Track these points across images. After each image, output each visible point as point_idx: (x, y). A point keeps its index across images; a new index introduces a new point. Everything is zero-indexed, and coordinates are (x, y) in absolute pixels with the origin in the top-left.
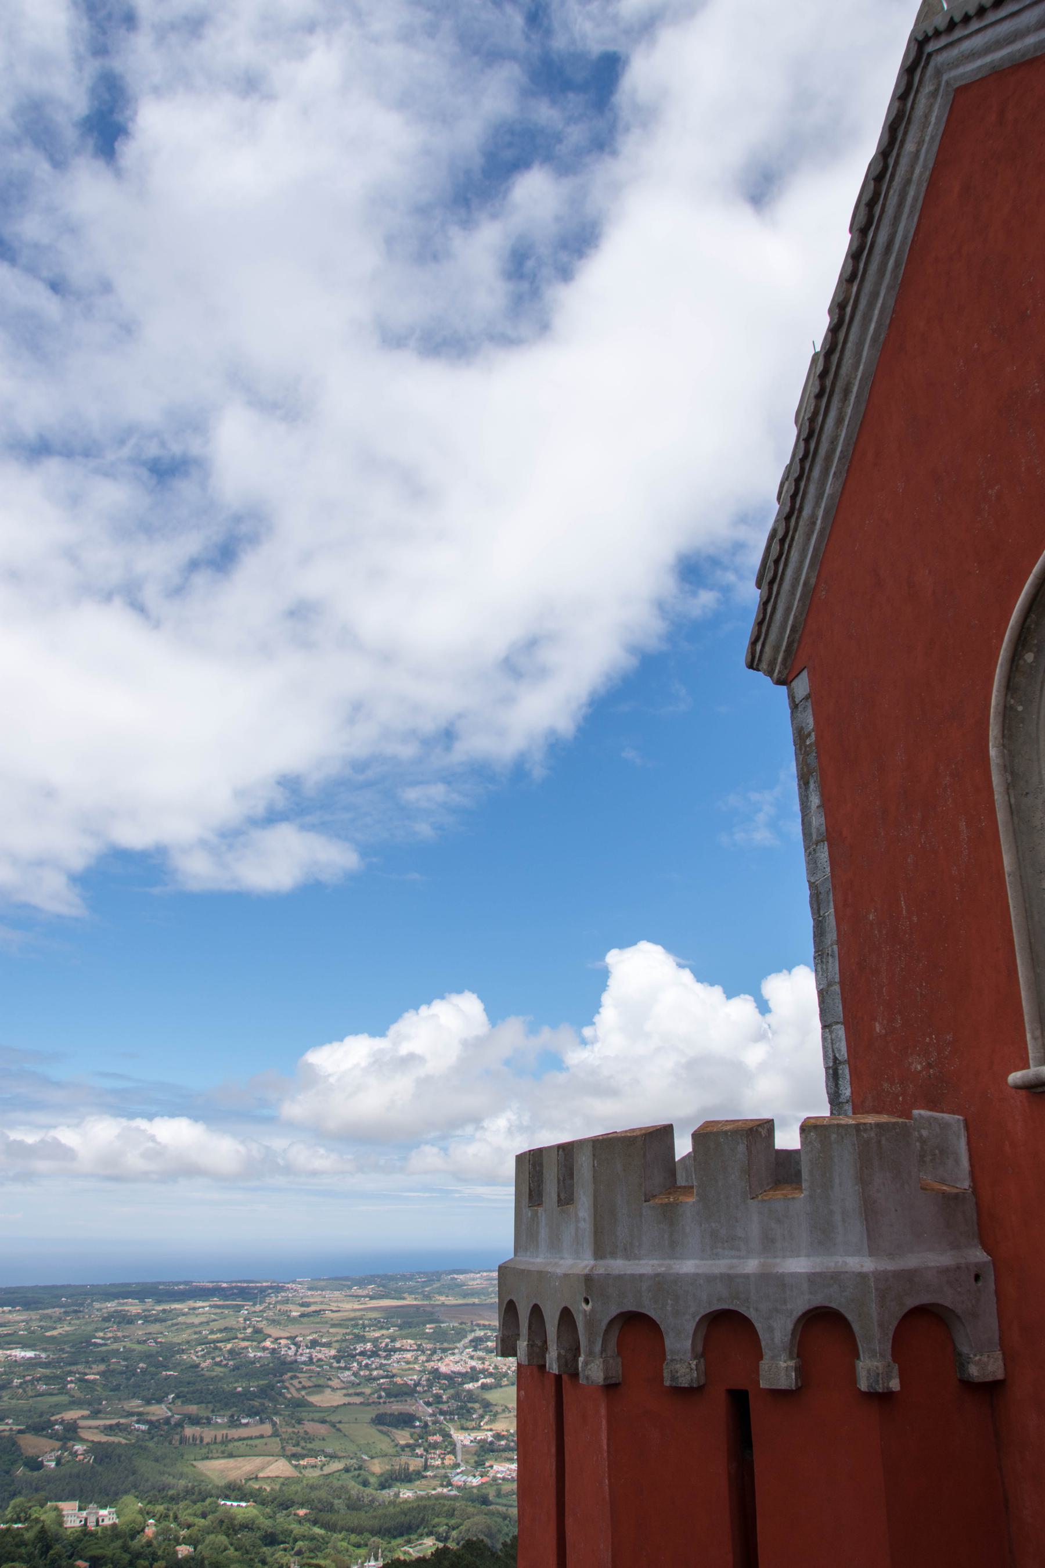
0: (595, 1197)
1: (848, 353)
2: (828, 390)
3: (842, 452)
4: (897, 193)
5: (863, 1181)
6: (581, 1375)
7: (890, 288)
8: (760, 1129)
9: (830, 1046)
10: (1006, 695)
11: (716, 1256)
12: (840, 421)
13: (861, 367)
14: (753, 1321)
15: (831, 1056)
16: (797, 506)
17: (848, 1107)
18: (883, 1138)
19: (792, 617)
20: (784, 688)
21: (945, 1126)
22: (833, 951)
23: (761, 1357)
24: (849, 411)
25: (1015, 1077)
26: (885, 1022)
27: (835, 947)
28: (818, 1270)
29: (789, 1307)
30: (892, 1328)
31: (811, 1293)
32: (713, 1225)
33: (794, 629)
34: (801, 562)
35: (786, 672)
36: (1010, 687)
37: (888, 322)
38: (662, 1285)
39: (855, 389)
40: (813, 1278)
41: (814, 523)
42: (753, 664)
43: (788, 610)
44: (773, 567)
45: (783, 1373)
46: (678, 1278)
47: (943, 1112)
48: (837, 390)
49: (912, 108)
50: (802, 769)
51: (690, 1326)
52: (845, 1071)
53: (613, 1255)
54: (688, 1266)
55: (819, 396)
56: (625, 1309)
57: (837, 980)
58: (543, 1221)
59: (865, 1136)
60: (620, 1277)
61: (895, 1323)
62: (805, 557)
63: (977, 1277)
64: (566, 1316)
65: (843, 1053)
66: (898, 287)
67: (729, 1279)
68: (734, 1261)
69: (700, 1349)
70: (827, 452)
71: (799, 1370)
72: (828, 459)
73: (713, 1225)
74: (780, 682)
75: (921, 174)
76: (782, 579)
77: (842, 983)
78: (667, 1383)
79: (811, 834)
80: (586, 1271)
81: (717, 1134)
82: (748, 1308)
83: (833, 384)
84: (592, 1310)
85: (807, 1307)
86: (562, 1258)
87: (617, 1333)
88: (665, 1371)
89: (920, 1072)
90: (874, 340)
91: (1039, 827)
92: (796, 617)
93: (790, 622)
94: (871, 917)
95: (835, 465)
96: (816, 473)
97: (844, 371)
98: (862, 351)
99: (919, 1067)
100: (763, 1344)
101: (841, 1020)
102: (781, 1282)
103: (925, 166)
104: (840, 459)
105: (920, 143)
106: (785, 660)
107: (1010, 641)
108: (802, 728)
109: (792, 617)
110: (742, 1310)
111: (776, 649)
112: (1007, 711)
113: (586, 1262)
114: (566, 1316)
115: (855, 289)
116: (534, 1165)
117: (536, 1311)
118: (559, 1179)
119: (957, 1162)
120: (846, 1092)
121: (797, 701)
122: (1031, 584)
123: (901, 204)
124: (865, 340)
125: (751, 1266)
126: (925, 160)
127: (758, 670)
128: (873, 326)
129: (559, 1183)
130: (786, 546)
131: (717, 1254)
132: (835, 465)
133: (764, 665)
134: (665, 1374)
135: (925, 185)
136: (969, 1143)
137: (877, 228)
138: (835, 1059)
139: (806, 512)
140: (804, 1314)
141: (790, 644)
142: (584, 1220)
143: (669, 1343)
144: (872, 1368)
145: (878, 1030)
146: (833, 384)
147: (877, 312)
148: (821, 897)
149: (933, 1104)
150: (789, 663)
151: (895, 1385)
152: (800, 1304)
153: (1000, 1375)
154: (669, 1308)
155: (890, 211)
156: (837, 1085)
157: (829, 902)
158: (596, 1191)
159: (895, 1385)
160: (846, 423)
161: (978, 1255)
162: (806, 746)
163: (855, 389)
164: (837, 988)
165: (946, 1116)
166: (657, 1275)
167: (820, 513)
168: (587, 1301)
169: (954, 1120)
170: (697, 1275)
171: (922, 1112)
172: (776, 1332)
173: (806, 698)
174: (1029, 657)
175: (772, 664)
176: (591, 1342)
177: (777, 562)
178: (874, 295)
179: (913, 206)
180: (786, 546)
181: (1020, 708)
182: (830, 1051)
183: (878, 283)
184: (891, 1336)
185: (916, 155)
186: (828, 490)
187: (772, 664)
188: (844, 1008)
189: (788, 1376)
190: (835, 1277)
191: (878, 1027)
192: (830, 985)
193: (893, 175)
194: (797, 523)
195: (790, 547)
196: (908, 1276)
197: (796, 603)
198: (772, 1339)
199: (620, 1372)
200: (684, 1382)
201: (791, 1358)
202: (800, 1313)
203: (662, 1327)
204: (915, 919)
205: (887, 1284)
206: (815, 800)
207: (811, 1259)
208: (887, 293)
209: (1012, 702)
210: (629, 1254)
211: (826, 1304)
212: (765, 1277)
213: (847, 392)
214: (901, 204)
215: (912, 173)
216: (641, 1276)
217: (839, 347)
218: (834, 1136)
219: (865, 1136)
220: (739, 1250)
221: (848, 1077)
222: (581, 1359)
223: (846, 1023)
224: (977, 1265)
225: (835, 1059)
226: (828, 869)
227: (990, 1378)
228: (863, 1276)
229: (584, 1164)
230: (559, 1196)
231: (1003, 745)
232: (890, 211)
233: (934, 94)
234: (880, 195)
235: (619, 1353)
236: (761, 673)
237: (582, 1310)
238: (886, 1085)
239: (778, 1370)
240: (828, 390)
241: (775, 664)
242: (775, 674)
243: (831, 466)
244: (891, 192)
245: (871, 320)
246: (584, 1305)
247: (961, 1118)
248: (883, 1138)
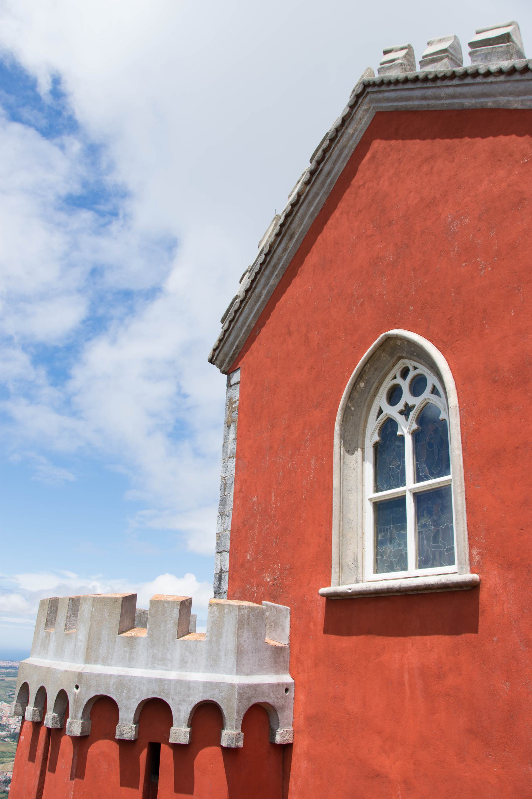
0: (90, 629)
1: (297, 218)
2: (283, 233)
3: (282, 265)
4: (339, 150)
5: (238, 635)
6: (67, 730)
7: (325, 193)
8: (186, 602)
9: (219, 562)
10: (348, 401)
11: (154, 668)
12: (285, 250)
13: (302, 227)
14: (170, 705)
15: (219, 568)
16: (254, 286)
17: (225, 595)
18: (251, 614)
19: (238, 341)
20: (225, 377)
21: (279, 611)
22: (229, 514)
23: (171, 725)
24: (291, 246)
25: (323, 590)
26: (253, 554)
27: (231, 512)
28: (209, 680)
29: (191, 699)
30: (243, 714)
31: (204, 693)
32: (155, 651)
33: (237, 347)
34: (249, 315)
35: (228, 368)
36: (350, 397)
37: (320, 209)
38: (122, 682)
39: (296, 236)
40: (207, 685)
41: (260, 297)
42: (211, 361)
43: (237, 337)
44: (233, 314)
46: (131, 679)
47: (278, 603)
48: (287, 235)
49: (355, 113)
50: (228, 418)
51: (135, 706)
52: (226, 577)
53: (96, 662)
54: (138, 672)
55: (277, 235)
56: (99, 694)
57: (229, 529)
58: (53, 638)
59: (242, 612)
60: (99, 675)
61: (245, 711)
62: (252, 312)
63: (287, 690)
64: (62, 696)
65: (226, 567)
66: (328, 194)
67: (160, 681)
68: (164, 671)
69: (137, 719)
70: (275, 263)
71: (192, 734)
72: (275, 267)
73: (155, 651)
74: (224, 372)
75: (353, 144)
76: (237, 321)
77: (232, 531)
78: (117, 737)
79: (227, 453)
80: (80, 670)
81: (164, 602)
82: (168, 698)
83: (286, 231)
84: (80, 693)
86: (63, 661)
87: (91, 707)
88: (117, 730)
89: (269, 582)
90: (312, 215)
91: (352, 468)
92: (240, 341)
93: (236, 343)
94: (254, 500)
95: (278, 270)
96: (267, 273)
97: (293, 226)
98: (304, 219)
99: (269, 580)
100: (174, 718)
101: (228, 550)
102: (188, 685)
103: (355, 142)
104: (281, 268)
105: (355, 130)
106: (229, 362)
107: (355, 374)
108: (232, 398)
109: (238, 341)
110: (165, 699)
111: (226, 355)
112: (346, 409)
113: (79, 665)
114: (62, 696)
115: (308, 188)
116: (51, 607)
117: (42, 691)
118: (67, 616)
119: (283, 630)
120: (225, 587)
121: (232, 384)
122: (372, 350)
123: (339, 156)
124: (307, 214)
125: (173, 675)
126: (356, 139)
127: (213, 364)
128: (312, 208)
129: (67, 618)
130: (243, 305)
131: (154, 667)
132: (278, 270)
133: (218, 362)
134: (117, 732)
135: (353, 150)
136: (291, 621)
137: (326, 163)
138: (221, 569)
139: (257, 291)
140: (198, 704)
141: (234, 354)
142: (81, 641)
143: (122, 714)
144: (231, 734)
145: (248, 558)
146: (286, 231)
147: (316, 202)
148: (227, 485)
149: (273, 599)
150: (231, 364)
151: (241, 744)
152: (197, 699)
153: (291, 742)
154: (124, 695)
155: (334, 157)
156: (220, 583)
157: (231, 489)
158: (91, 626)
159: (241, 744)
160: (288, 251)
161: (287, 679)
162: (232, 408)
163: (296, 236)
164: (228, 533)
165: (281, 606)
166: (120, 676)
167: (264, 292)
168: (77, 687)
169: (285, 609)
170: (143, 677)
171: (268, 603)
172: (181, 713)
173: (237, 383)
174: (362, 385)
175: (222, 362)
176: (76, 711)
177: (236, 312)
178: (317, 194)
179: (345, 158)
180: (243, 305)
181: (353, 409)
182: (219, 565)
183: (320, 189)
184: (242, 718)
185: (353, 135)
186: (272, 282)
187: (222, 362)
188: (231, 543)
189: (185, 736)
190: (217, 685)
191: (248, 556)
192: (224, 531)
193: (339, 141)
194: (251, 295)
195: (245, 306)
196: (255, 687)
197: (242, 334)
198: (179, 716)
199: (90, 729)
200: (127, 737)
201: (188, 727)
202: (196, 703)
203: (119, 705)
204: (279, 504)
205: (244, 691)
206: (232, 435)
207: (206, 674)
208: (323, 195)
209: (350, 404)
210: (105, 661)
211: (211, 699)
212: (180, 682)
213: (292, 236)
214: (339, 156)
215: (348, 143)
216: (111, 675)
217: (294, 214)
218: (226, 610)
219: (242, 612)
220: (167, 666)
221: (227, 580)
222: (69, 720)
223: (231, 552)
224: (287, 684)
225: (221, 569)
226: (234, 472)
227: (286, 743)
228: (232, 686)
229: (85, 609)
230: (66, 626)
231: (342, 425)
232: (334, 157)
233: (367, 111)
234: (330, 148)
235: (91, 718)
236: (215, 366)
237: (72, 693)
238: (248, 587)
239: (180, 732)
240: (283, 233)
241: (224, 363)
242: (223, 368)
243: (276, 271)
244: (336, 148)
245: (312, 205)
246: (75, 689)
247: (289, 608)
248: (251, 614)
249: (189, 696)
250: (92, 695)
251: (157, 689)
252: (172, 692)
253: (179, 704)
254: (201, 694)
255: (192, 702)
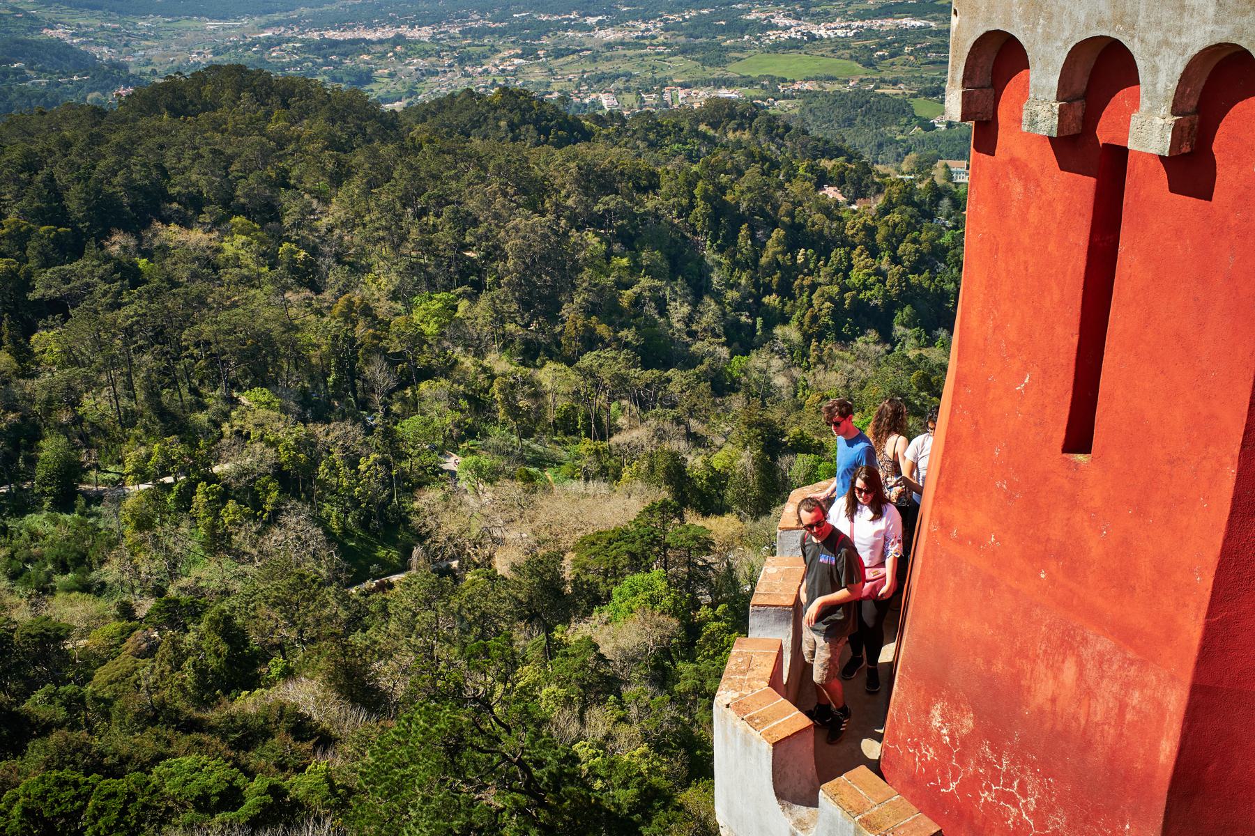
29: (1184, 40)
31: (1216, 22)
45: (1157, 132)
82: (1133, 37)
85: (1207, 43)
110: (1124, 40)
172: (1160, 76)
198: (1154, 85)
202: (1196, 51)
249: (1180, 33)
250: (981, 32)
251: (1108, 14)
252: (1141, 23)
253: (1155, 55)
254: (1209, 28)
255: (1185, 50)
